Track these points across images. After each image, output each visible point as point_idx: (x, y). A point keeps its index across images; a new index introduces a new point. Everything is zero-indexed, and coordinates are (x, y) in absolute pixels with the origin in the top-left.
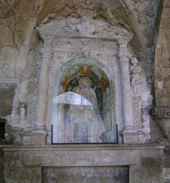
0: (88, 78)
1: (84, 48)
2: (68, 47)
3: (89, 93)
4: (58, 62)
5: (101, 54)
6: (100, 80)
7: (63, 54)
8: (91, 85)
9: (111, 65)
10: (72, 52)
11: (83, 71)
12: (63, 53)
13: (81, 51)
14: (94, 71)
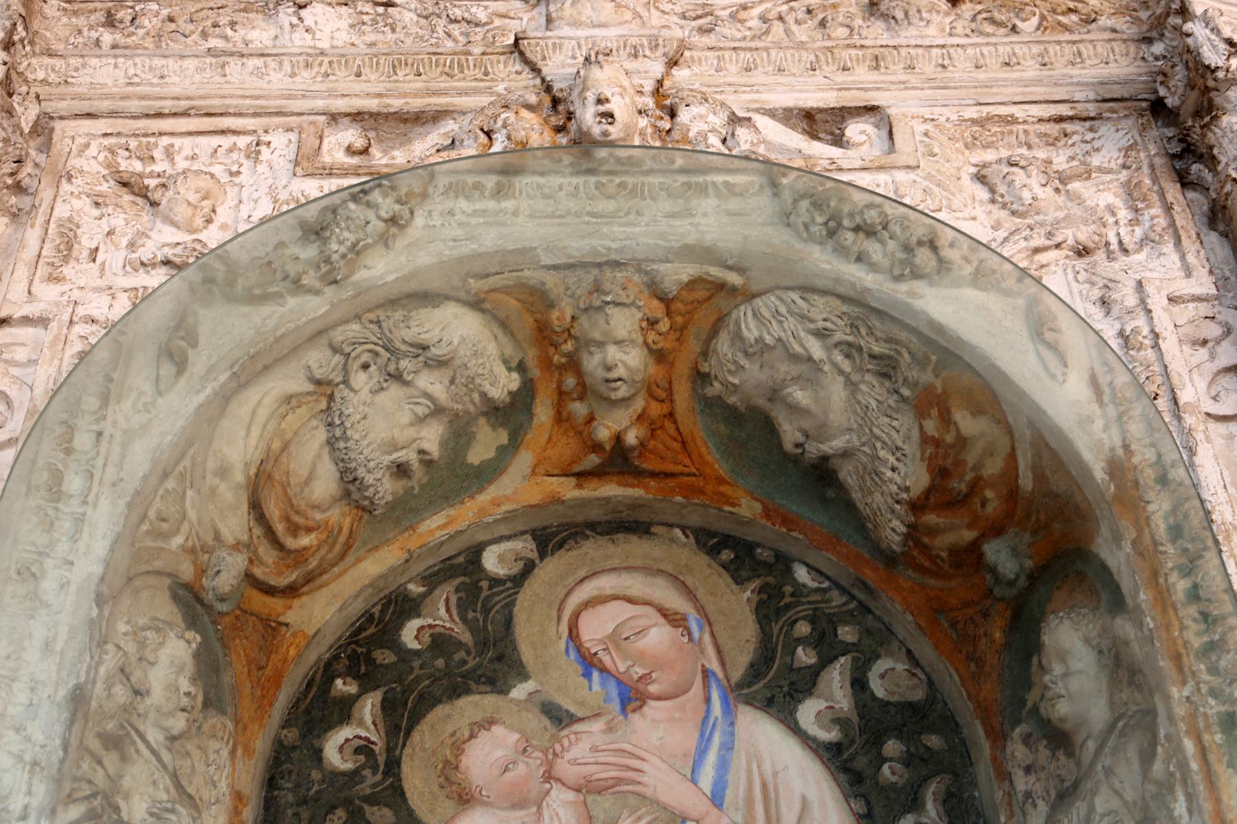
0: (684, 553)
1: (576, 24)
2: (300, 40)
3: (717, 799)
4: (132, 246)
5: (871, 109)
6: (893, 530)
7: (226, 141)
8: (741, 660)
9: (1068, 235)
10: (372, 104)
11: (579, 409)
12: (223, 132)
13: (527, 78)
14: (775, 394)
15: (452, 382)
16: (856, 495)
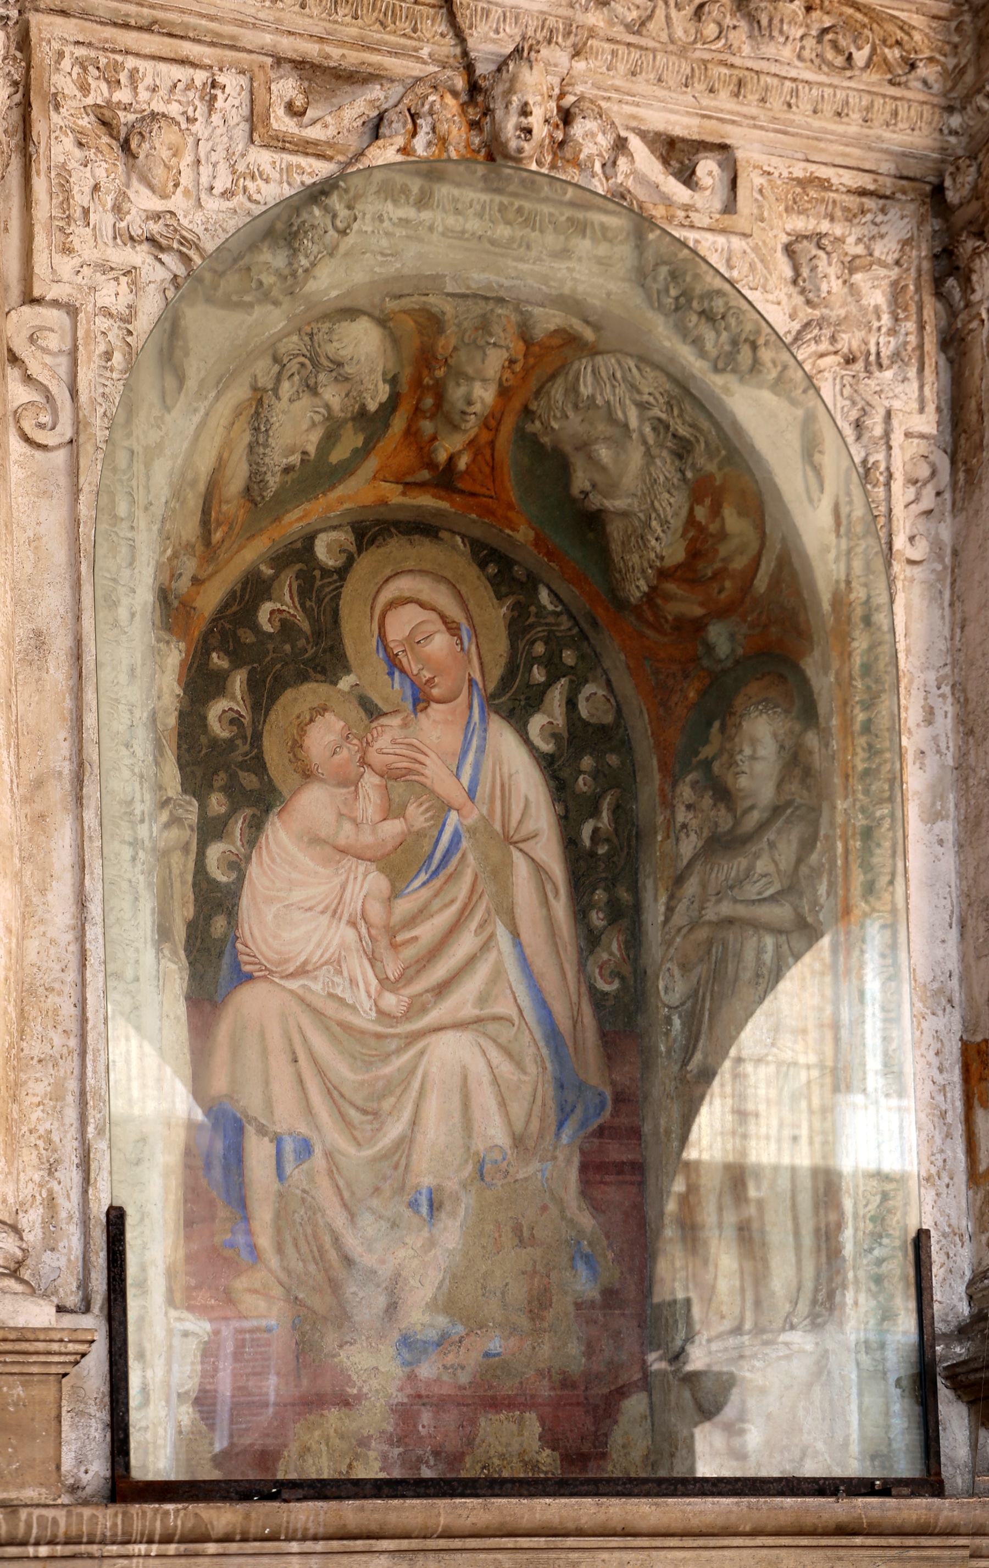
15: (347, 395)
16: (615, 547)
